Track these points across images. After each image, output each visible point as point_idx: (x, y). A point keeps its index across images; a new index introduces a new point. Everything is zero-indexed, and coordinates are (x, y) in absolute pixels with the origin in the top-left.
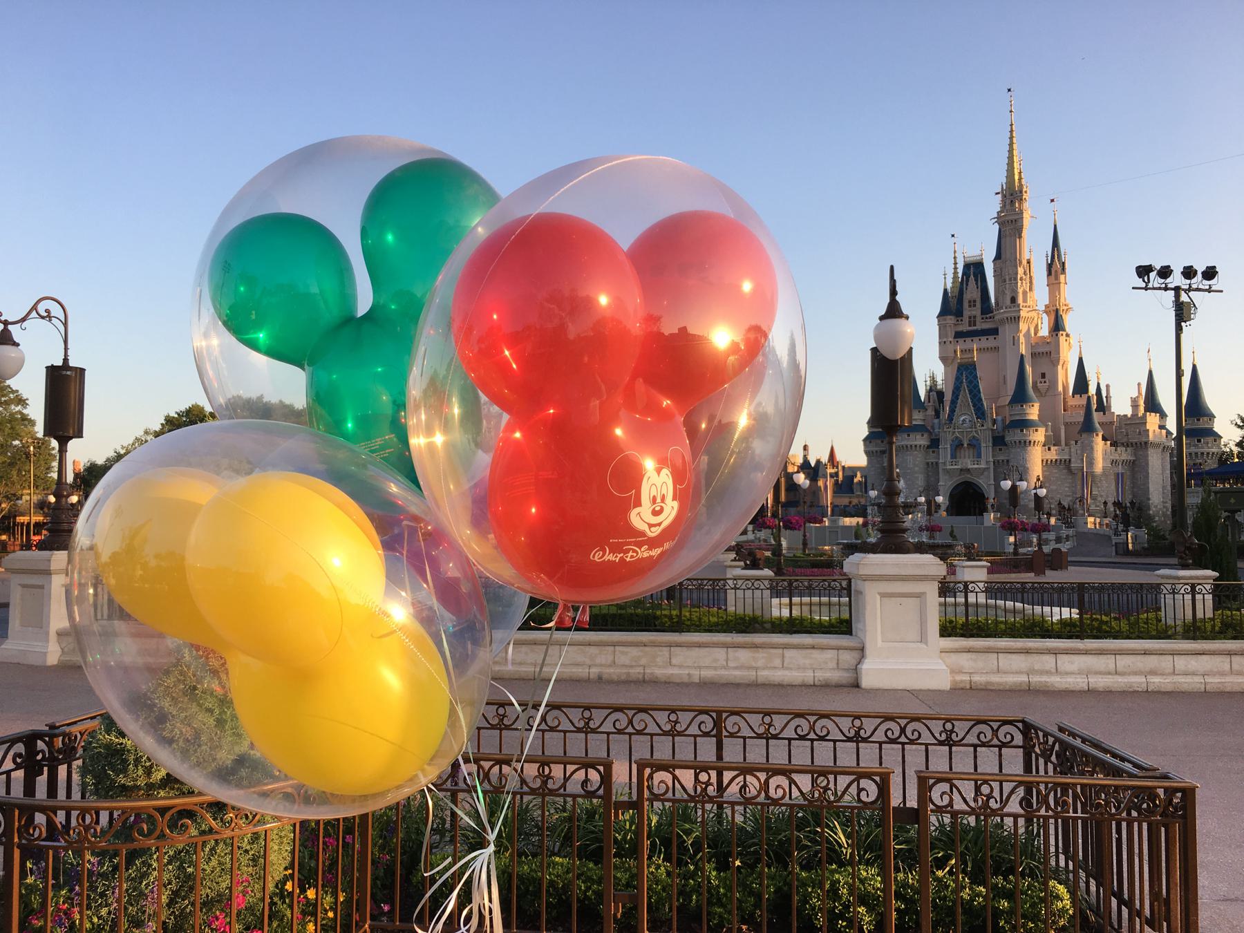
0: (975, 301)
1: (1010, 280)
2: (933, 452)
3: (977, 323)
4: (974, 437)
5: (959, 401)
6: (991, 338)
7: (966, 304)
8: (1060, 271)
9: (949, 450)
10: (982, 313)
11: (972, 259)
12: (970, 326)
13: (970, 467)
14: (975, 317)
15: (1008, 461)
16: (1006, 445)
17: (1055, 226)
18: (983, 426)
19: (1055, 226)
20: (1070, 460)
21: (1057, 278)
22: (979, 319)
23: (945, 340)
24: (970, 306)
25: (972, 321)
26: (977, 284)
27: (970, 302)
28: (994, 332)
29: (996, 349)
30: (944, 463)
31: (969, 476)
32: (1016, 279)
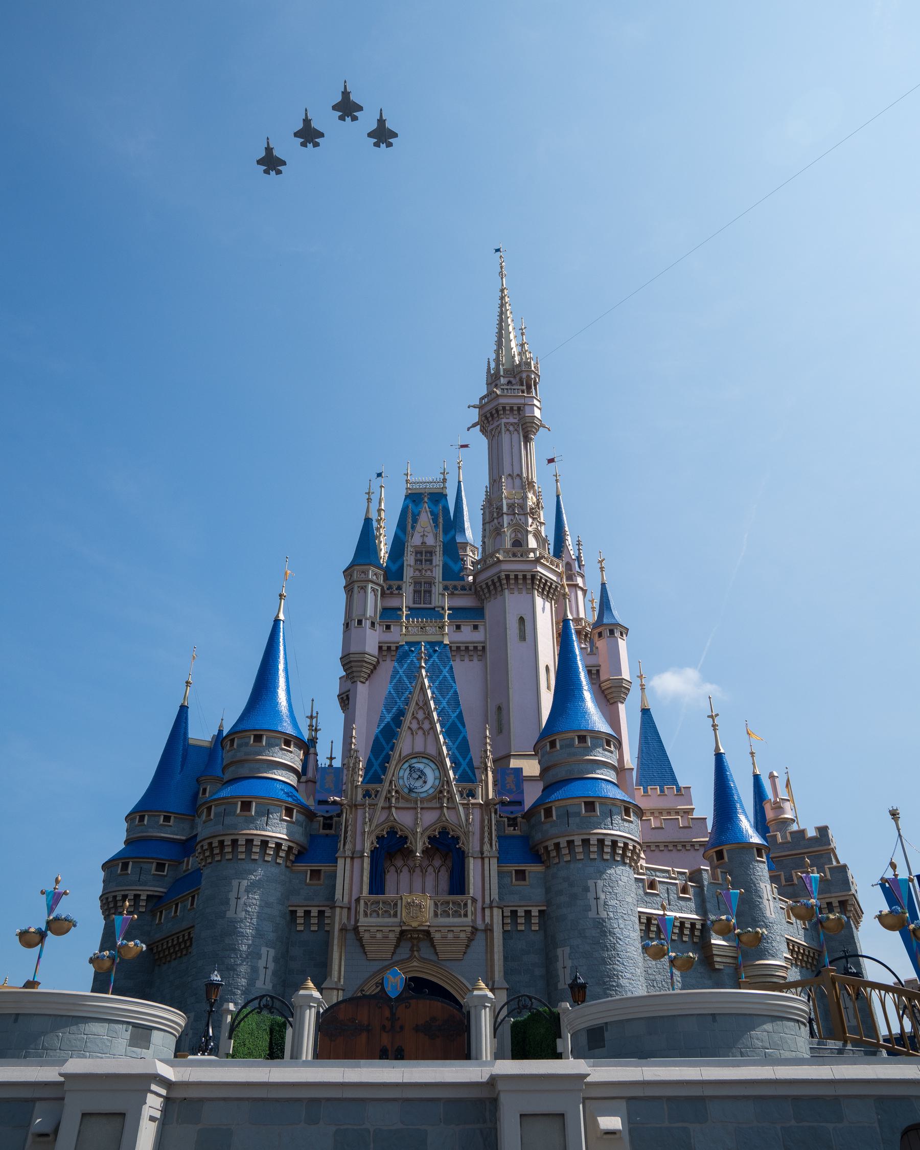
0: (431, 553)
1: (511, 506)
7: (409, 559)
9: (367, 862)
18: (472, 794)
27: (417, 553)
29: (476, 651)
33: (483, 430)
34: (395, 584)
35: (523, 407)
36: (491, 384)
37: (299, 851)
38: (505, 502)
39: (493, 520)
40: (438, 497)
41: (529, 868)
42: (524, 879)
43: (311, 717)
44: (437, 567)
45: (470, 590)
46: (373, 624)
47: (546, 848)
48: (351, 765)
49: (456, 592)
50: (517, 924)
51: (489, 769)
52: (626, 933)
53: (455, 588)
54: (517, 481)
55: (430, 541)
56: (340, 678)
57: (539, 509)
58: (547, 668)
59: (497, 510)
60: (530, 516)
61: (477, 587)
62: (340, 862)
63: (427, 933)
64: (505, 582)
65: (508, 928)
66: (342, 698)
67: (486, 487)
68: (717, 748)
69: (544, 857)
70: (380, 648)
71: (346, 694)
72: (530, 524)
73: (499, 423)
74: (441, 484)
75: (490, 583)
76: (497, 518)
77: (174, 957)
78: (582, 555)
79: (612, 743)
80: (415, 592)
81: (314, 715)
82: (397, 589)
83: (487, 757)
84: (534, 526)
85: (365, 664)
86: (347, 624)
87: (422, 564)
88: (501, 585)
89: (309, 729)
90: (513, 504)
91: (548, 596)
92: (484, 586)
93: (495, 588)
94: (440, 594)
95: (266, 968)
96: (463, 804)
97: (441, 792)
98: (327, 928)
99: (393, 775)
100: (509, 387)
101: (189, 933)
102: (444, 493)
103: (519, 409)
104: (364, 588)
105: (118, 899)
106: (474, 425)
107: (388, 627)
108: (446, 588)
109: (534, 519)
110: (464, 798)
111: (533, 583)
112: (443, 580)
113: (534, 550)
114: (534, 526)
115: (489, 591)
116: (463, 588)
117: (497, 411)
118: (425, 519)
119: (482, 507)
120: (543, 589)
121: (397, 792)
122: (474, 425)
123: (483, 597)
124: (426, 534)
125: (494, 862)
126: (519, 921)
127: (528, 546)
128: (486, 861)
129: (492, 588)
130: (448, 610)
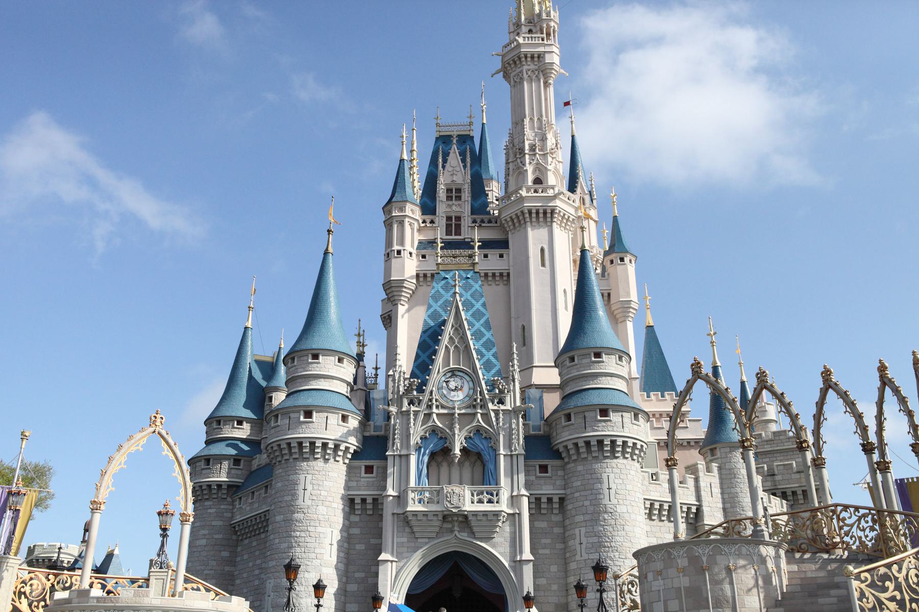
0: (459, 190)
1: (533, 148)
2: (369, 469)
4: (478, 431)
5: (445, 340)
10: (473, 212)
13: (469, 506)
14: (458, 218)
15: (562, 500)
16: (557, 455)
17: (573, 137)
18: (501, 402)
19: (573, 137)
20: (699, 509)
24: (449, 198)
25: (453, 224)
26: (464, 161)
29: (504, 277)
30: (401, 499)
31: (464, 536)
33: (506, 76)
34: (428, 218)
35: (544, 55)
36: (513, 32)
37: (355, 450)
38: (527, 143)
39: (517, 160)
40: (464, 139)
41: (551, 463)
43: (359, 335)
44: (466, 203)
45: (496, 222)
46: (411, 254)
47: (566, 447)
48: (397, 378)
49: (483, 225)
50: (540, 508)
51: (516, 380)
52: (633, 516)
53: (483, 221)
55: (458, 179)
56: (382, 301)
57: (557, 149)
58: (565, 291)
59: (520, 151)
60: (550, 156)
61: (502, 219)
62: (390, 460)
63: (466, 517)
64: (527, 215)
65: (533, 512)
66: (385, 317)
67: (510, 129)
68: (715, 362)
69: (564, 455)
71: (388, 314)
72: (549, 163)
73: (519, 70)
74: (468, 127)
75: (514, 217)
76: (520, 158)
77: (253, 534)
78: (594, 189)
79: (623, 358)
81: (361, 333)
82: (430, 223)
83: (514, 370)
84: (553, 165)
85: (404, 290)
86: (388, 254)
87: (452, 200)
88: (524, 219)
89: (357, 346)
90: (535, 145)
91: (565, 228)
92: (509, 219)
93: (519, 222)
94: (469, 226)
95: (331, 545)
96: (493, 410)
97: (475, 400)
98: (380, 513)
99: (433, 386)
100: (529, 35)
101: (265, 515)
102: (471, 135)
103: (539, 57)
104: (401, 223)
105: (203, 488)
106: (497, 72)
108: (474, 221)
109: (553, 158)
110: (495, 405)
111: (552, 217)
112: (472, 213)
113: (553, 187)
114: (553, 165)
115: (514, 224)
116: (490, 222)
117: (520, 58)
118: (454, 159)
119: (505, 148)
120: (561, 222)
121: (436, 400)
122: (497, 72)
123: (508, 229)
125: (521, 460)
126: (543, 506)
127: (547, 183)
128: (515, 458)
129: (515, 221)
130: (478, 242)
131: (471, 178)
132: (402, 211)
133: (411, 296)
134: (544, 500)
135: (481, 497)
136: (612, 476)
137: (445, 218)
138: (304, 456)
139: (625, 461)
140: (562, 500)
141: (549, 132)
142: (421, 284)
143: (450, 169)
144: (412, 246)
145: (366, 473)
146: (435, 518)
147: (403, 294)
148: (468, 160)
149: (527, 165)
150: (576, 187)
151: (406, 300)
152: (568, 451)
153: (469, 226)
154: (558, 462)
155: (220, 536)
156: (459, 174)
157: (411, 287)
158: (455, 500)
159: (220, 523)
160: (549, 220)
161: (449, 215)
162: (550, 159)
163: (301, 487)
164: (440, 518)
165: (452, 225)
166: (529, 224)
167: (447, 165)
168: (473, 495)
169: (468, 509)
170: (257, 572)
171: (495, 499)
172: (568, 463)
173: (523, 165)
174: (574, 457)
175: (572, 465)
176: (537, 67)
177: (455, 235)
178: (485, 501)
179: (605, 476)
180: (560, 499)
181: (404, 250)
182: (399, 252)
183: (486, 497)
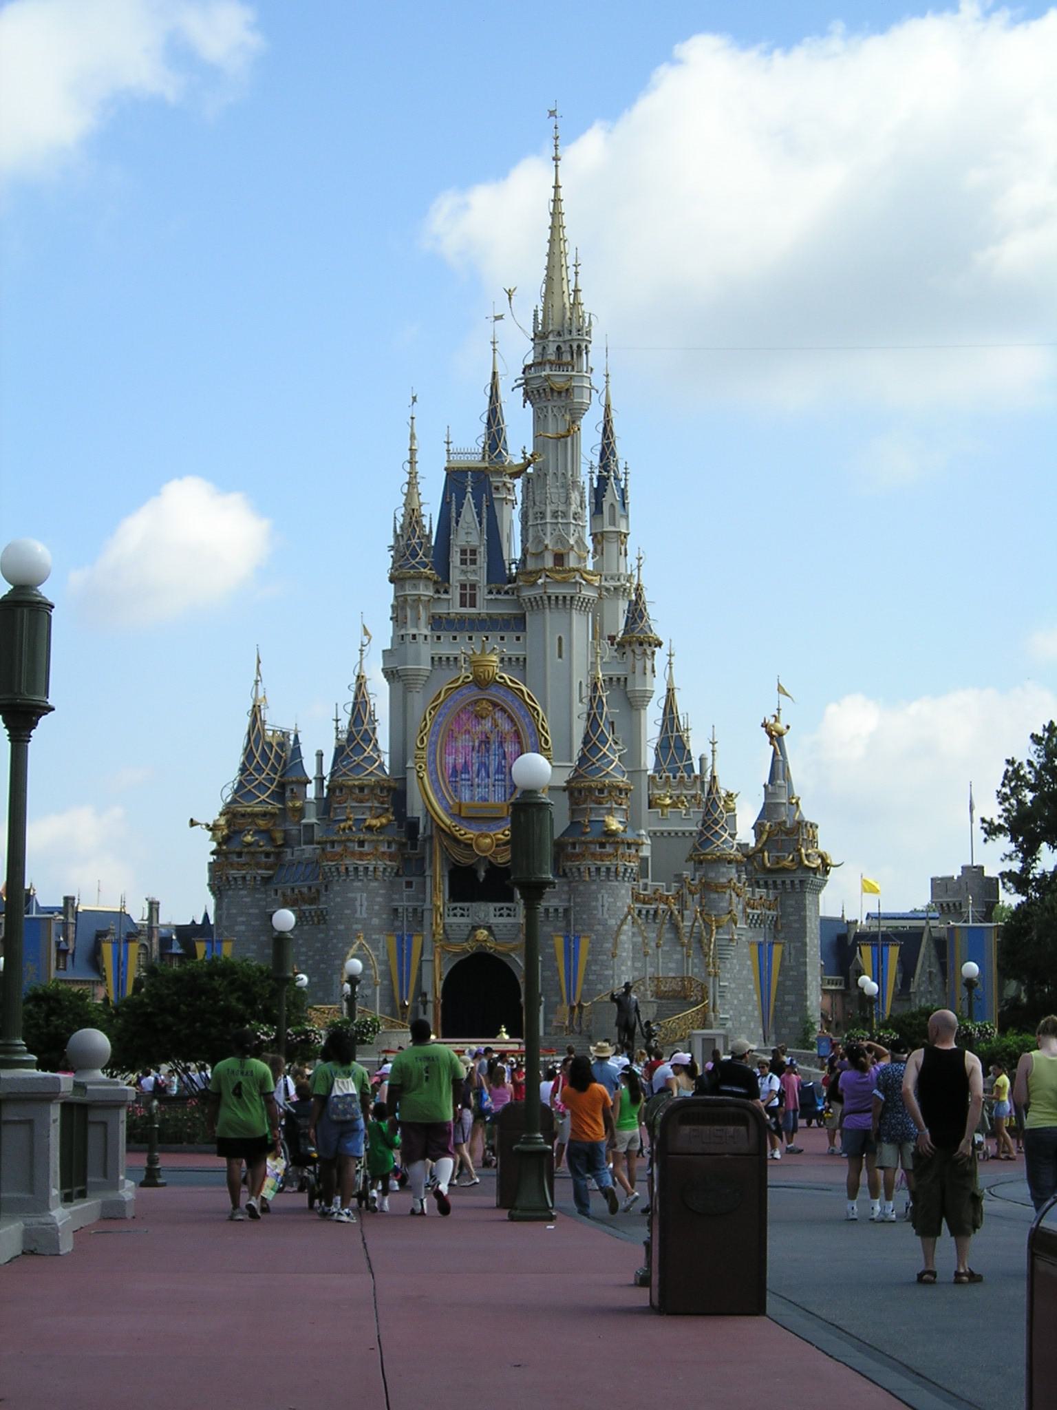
0: (473, 552)
1: (555, 514)
2: (409, 884)
3: (479, 601)
6: (510, 636)
7: (456, 558)
8: (618, 506)
11: (464, 458)
12: (463, 605)
14: (473, 587)
21: (613, 523)
22: (482, 594)
23: (413, 631)
24: (463, 562)
26: (479, 514)
27: (463, 552)
28: (518, 623)
32: (565, 515)
42: (554, 888)
45: (513, 593)
46: (426, 636)
49: (499, 597)
53: (499, 592)
54: (561, 479)
64: (546, 602)
69: (569, 875)
70: (433, 658)
72: (572, 532)
73: (545, 404)
75: (533, 600)
80: (461, 594)
84: (576, 535)
87: (466, 564)
88: (543, 604)
90: (557, 512)
92: (527, 600)
93: (538, 606)
107: (439, 638)
108: (490, 592)
112: (489, 582)
114: (576, 535)
124: (470, 531)
126: (550, 915)
129: (534, 604)
131: (487, 536)
132: (416, 587)
133: (426, 681)
134: (551, 910)
135: (502, 911)
136: (606, 896)
137: (459, 588)
138: (360, 878)
139: (617, 883)
140: (566, 911)
141: (573, 490)
142: (436, 667)
143: (465, 525)
144: (427, 627)
145: (406, 888)
146: (466, 929)
147: (419, 682)
148: (485, 515)
149: (549, 534)
150: (605, 491)
151: (421, 686)
152: (572, 873)
153: (484, 599)
154: (564, 880)
155: (258, 923)
156: (474, 532)
157: (426, 668)
158: (482, 915)
159: (256, 911)
160: (568, 607)
161: (465, 583)
162: (572, 527)
163: (358, 903)
164: (470, 928)
165: (466, 594)
166: (547, 611)
167: (461, 519)
168: (495, 910)
169: (491, 921)
170: (303, 958)
171: (512, 913)
172: (572, 882)
173: (544, 534)
174: (577, 879)
175: (574, 884)
176: (563, 404)
177: (471, 606)
178: (505, 914)
179: (600, 896)
180: (564, 909)
181: (420, 634)
182: (414, 637)
183: (505, 912)
